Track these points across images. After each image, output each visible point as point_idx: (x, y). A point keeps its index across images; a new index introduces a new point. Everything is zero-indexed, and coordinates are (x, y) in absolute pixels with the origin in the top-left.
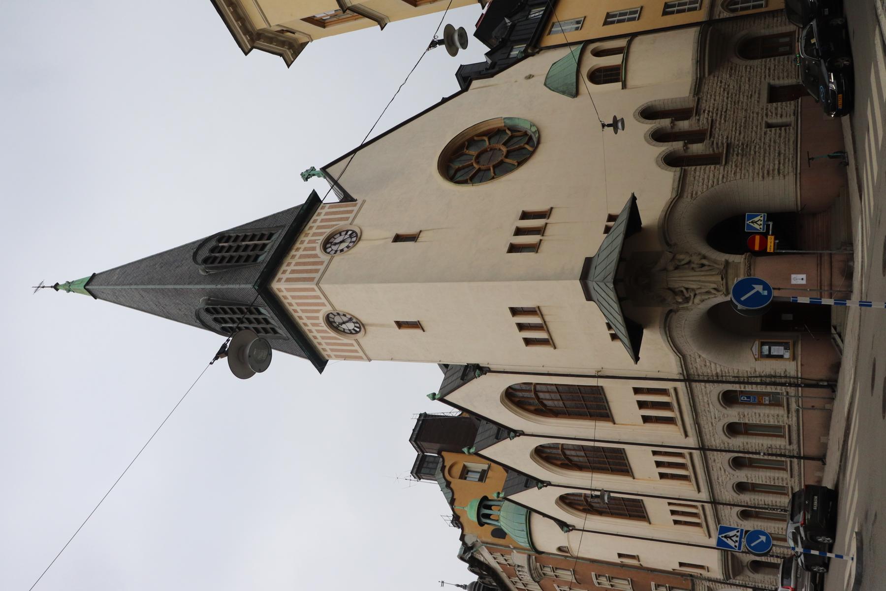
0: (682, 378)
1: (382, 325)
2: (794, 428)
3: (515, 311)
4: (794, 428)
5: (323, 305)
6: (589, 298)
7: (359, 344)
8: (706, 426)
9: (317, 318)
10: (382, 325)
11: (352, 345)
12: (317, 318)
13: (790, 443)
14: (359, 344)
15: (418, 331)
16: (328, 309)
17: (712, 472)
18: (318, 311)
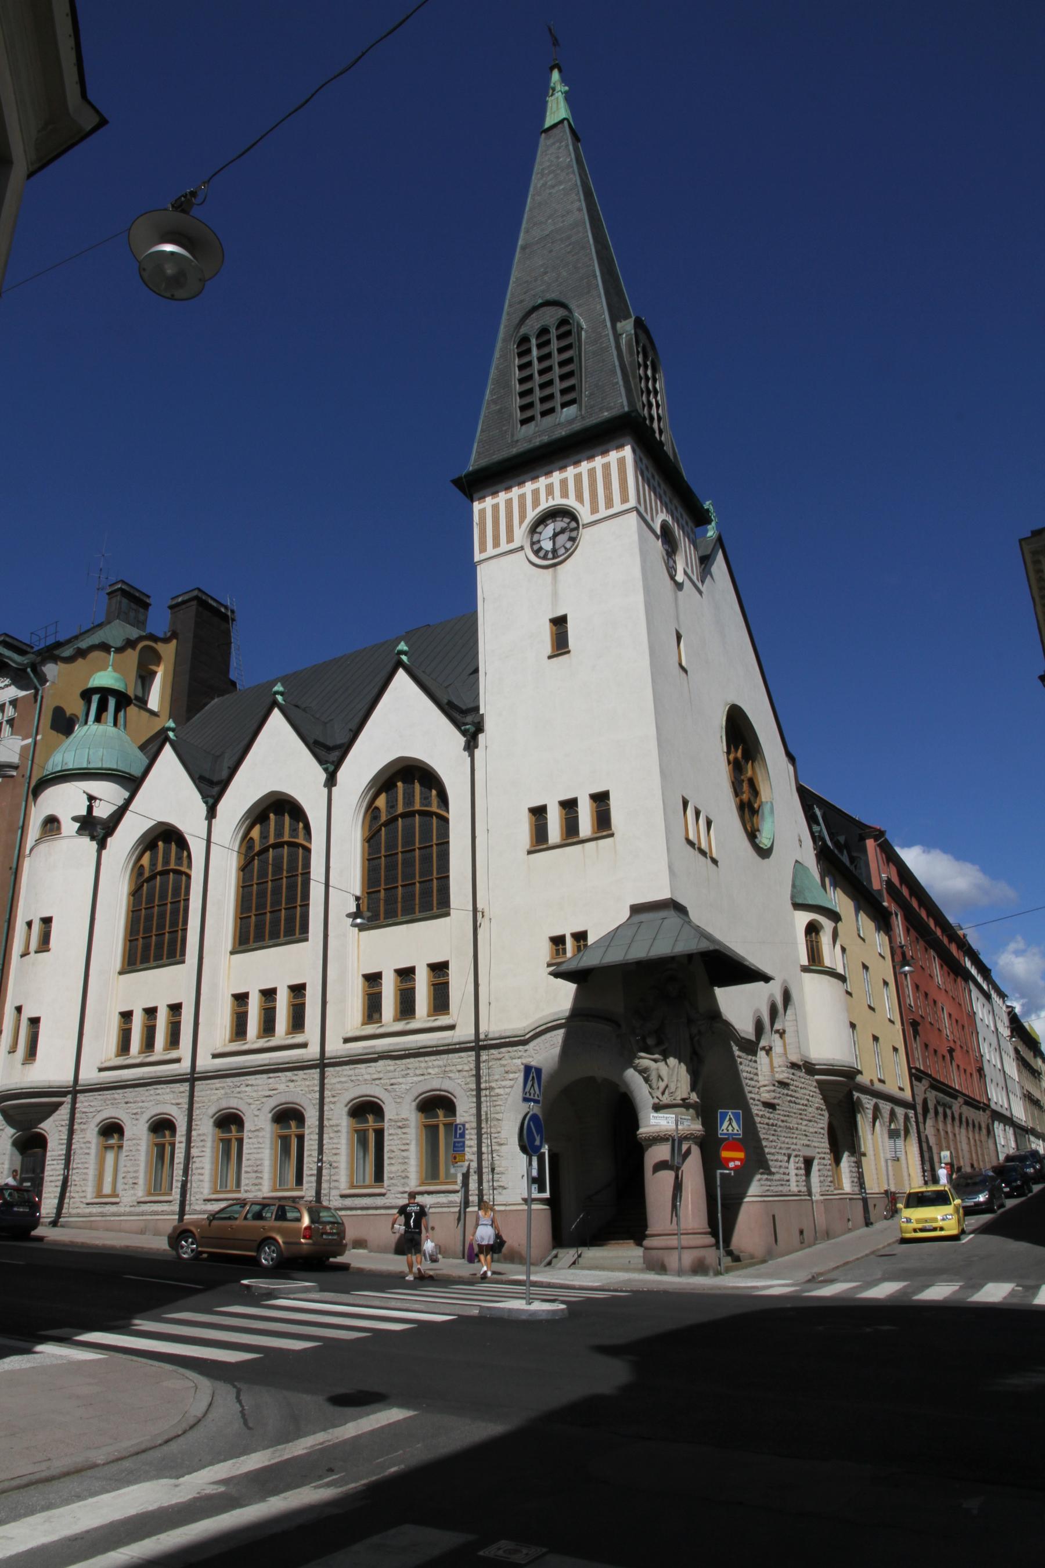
0: (482, 1036)
1: (555, 594)
2: (379, 1201)
3: (601, 799)
4: (379, 1201)
5: (594, 510)
6: (636, 909)
7: (511, 552)
8: (370, 1070)
9: (565, 494)
10: (555, 594)
11: (510, 539)
12: (565, 494)
13: (343, 1196)
14: (511, 552)
15: (547, 648)
16: (584, 514)
17: (265, 1076)
18: (580, 498)
